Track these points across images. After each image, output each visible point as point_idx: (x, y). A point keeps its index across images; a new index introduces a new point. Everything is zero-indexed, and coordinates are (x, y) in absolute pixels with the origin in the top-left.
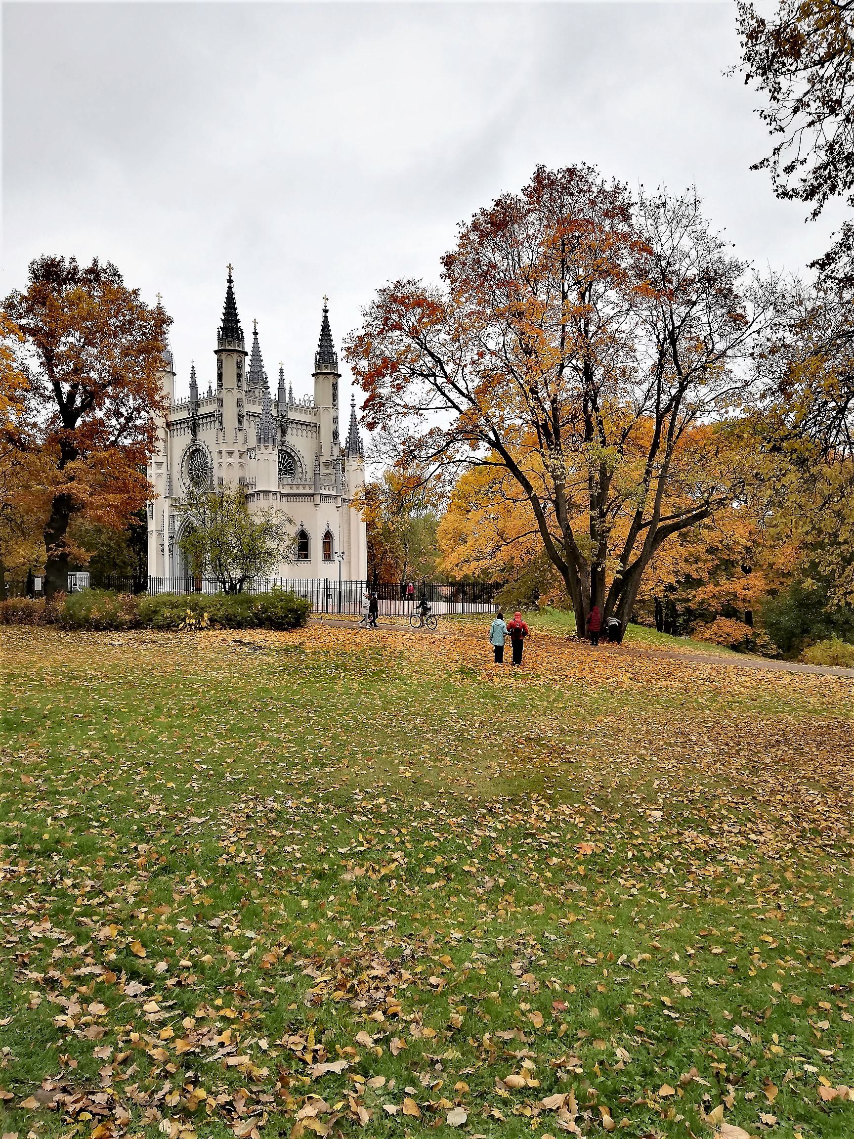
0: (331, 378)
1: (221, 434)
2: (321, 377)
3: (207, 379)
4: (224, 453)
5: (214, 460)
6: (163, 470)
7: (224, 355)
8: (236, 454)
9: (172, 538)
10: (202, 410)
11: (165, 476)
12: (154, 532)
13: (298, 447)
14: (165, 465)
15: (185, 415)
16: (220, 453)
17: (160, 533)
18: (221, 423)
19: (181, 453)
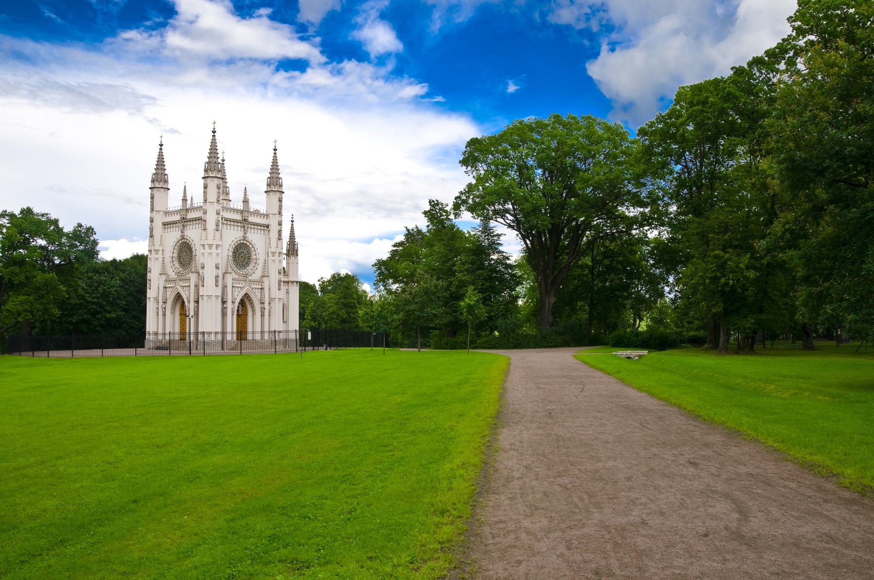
0: (278, 194)
1: (204, 233)
2: (272, 193)
3: (196, 195)
4: (206, 246)
5: (198, 250)
6: (160, 255)
7: (209, 180)
8: (214, 247)
9: (165, 303)
10: (191, 215)
11: (161, 259)
12: (152, 300)
13: (253, 242)
14: (161, 252)
15: (177, 218)
16: (203, 245)
17: (157, 300)
18: (205, 226)
19: (173, 244)
